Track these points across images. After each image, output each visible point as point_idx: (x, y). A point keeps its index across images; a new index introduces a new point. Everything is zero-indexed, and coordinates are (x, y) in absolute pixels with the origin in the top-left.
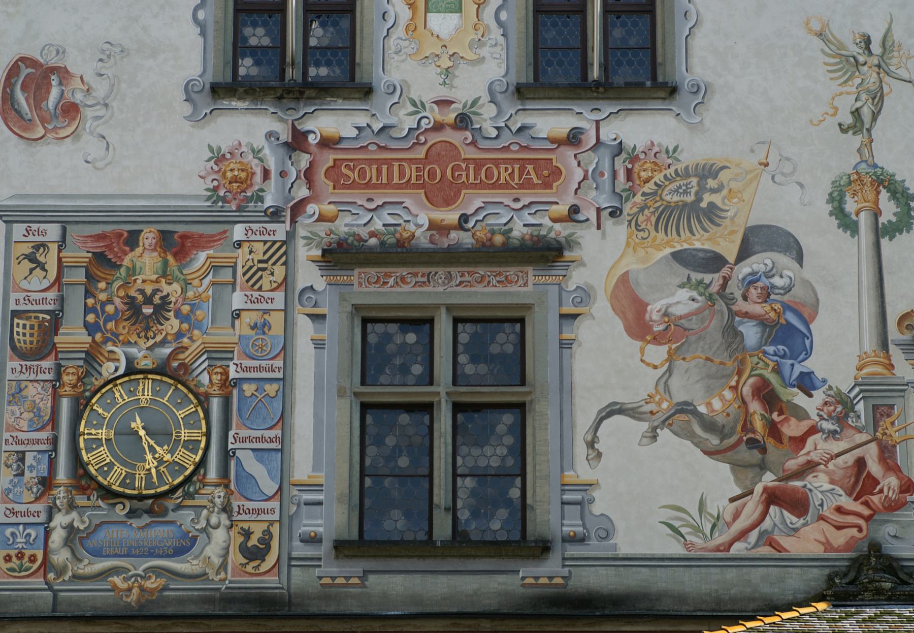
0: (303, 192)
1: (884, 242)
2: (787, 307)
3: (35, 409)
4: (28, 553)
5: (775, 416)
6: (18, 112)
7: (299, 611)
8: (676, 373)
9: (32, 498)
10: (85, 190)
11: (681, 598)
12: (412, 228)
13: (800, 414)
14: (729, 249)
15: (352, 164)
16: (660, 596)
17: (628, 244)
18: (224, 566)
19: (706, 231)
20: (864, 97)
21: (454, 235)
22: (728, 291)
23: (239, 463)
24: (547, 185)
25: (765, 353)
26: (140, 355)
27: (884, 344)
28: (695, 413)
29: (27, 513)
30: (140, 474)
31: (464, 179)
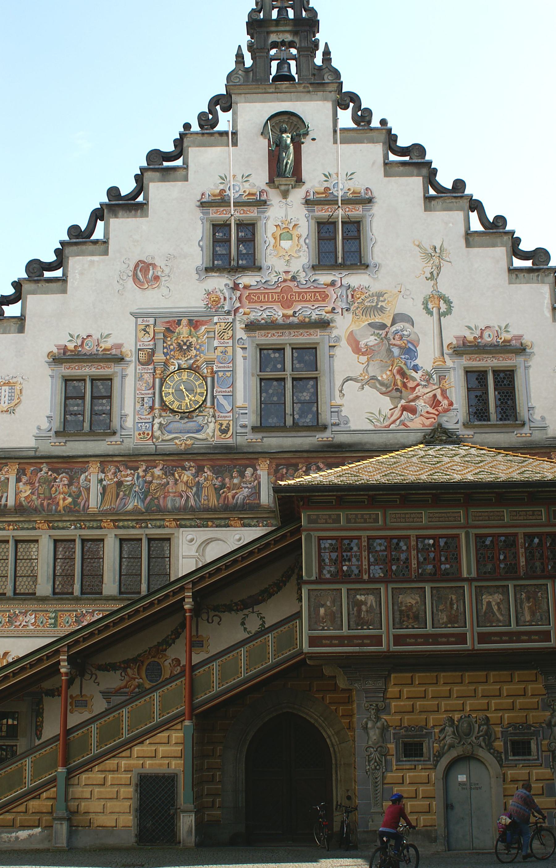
0: (238, 305)
1: (442, 318)
2: (408, 342)
4: (146, 432)
5: (405, 380)
6: (139, 279)
7: (240, 451)
8: (370, 366)
9: (147, 413)
10: (162, 306)
11: (373, 444)
12: (276, 316)
13: (414, 379)
14: (388, 322)
16: (365, 444)
17: (352, 321)
18: (213, 436)
19: (380, 315)
20: (434, 267)
21: (291, 318)
22: (388, 336)
24: (324, 300)
25: (401, 358)
26: (183, 363)
27: (443, 355)
28: (377, 379)
29: (146, 419)
30: (184, 404)
31: (294, 299)
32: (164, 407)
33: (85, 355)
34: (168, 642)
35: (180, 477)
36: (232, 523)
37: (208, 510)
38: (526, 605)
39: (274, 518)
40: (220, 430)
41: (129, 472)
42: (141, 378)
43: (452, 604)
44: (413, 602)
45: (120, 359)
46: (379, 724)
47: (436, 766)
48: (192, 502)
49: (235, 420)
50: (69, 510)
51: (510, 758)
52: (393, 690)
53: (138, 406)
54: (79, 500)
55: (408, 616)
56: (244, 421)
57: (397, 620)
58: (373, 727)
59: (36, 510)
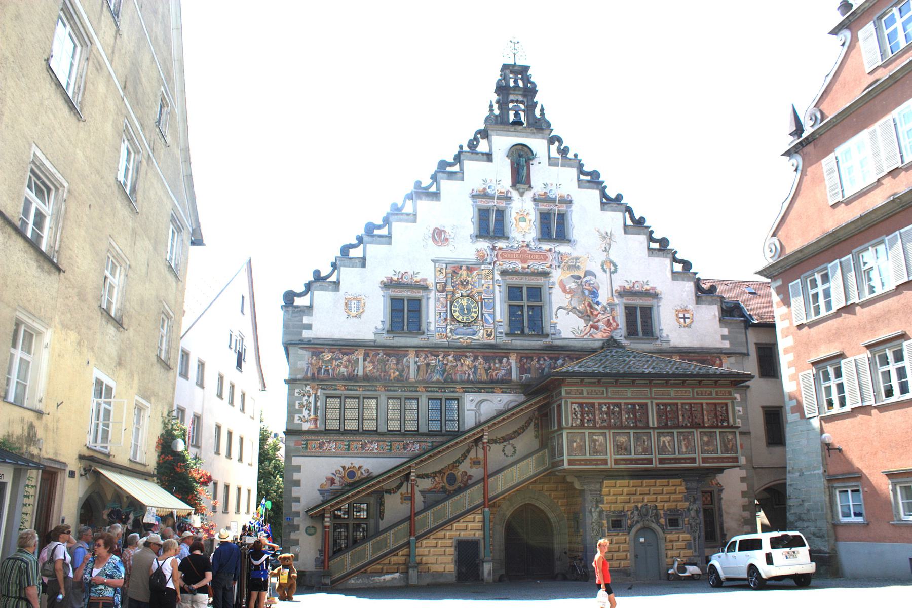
0: (496, 259)
2: (594, 288)
3: (443, 304)
11: (574, 347)
13: (596, 310)
14: (582, 276)
15: (505, 254)
18: (483, 338)
21: (527, 270)
23: (485, 317)
24: (545, 260)
27: (612, 296)
32: (453, 318)
33: (404, 284)
34: (459, 461)
35: (464, 362)
36: (496, 390)
37: (481, 382)
38: (683, 443)
39: (520, 389)
40: (487, 335)
41: (433, 357)
42: (439, 300)
43: (644, 442)
44: (624, 440)
45: (425, 288)
46: (598, 510)
47: (629, 533)
48: (472, 377)
49: (495, 329)
50: (397, 380)
51: (669, 528)
52: (605, 490)
53: (437, 318)
54: (403, 374)
55: (621, 448)
56: (500, 330)
57: (616, 450)
58: (595, 511)
59: (376, 379)
